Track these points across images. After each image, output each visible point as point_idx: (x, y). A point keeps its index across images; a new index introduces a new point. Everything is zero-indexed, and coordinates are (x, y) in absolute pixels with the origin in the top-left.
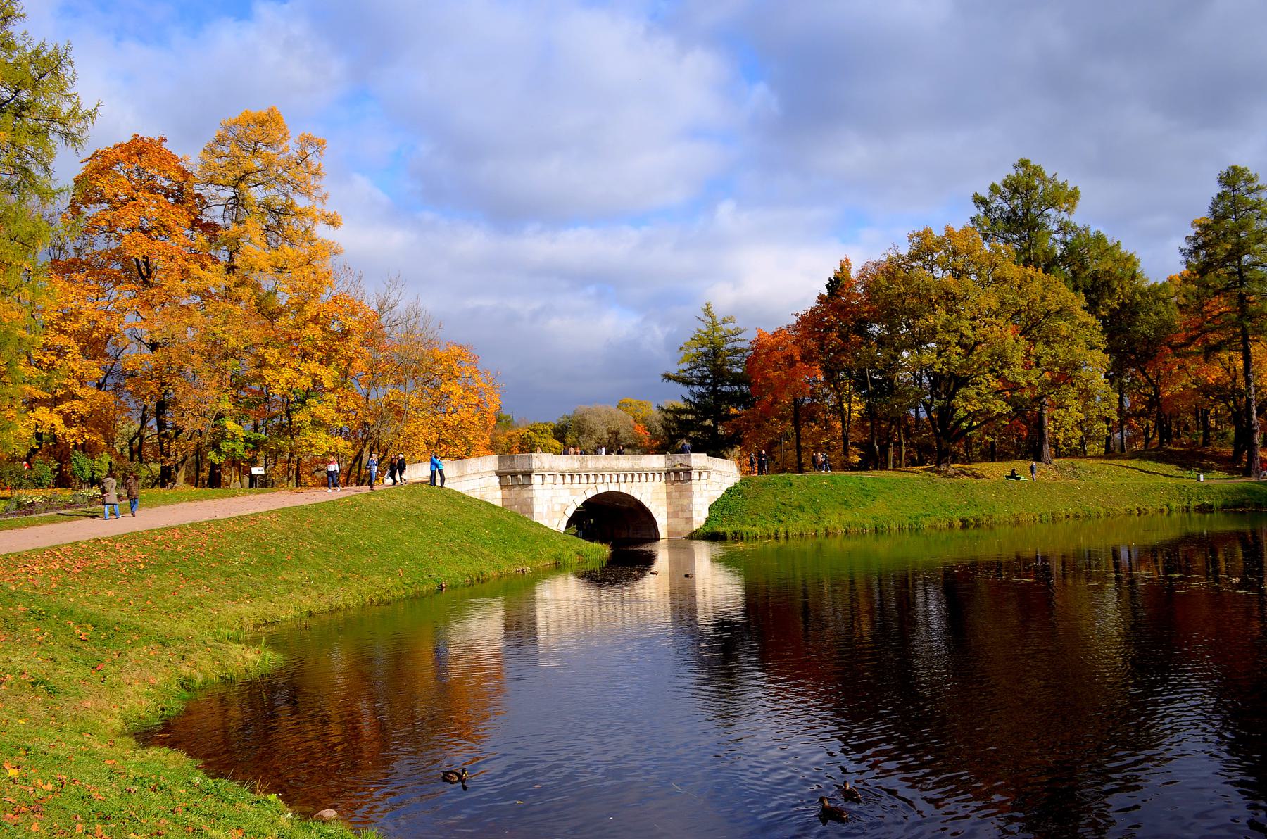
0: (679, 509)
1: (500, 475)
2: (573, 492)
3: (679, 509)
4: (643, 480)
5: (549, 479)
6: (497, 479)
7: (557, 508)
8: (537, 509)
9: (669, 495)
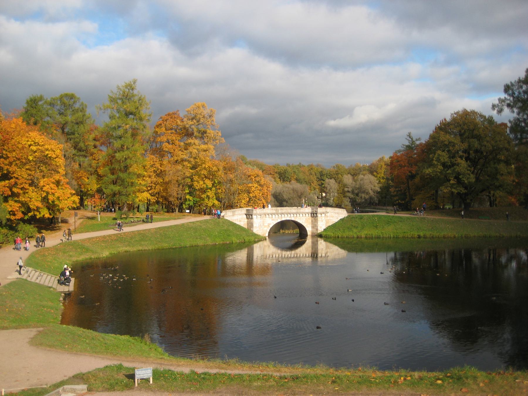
0: (315, 225)
1: (246, 215)
2: (273, 220)
3: (315, 225)
4: (302, 215)
7: (266, 224)
8: (254, 225)
9: (312, 221)
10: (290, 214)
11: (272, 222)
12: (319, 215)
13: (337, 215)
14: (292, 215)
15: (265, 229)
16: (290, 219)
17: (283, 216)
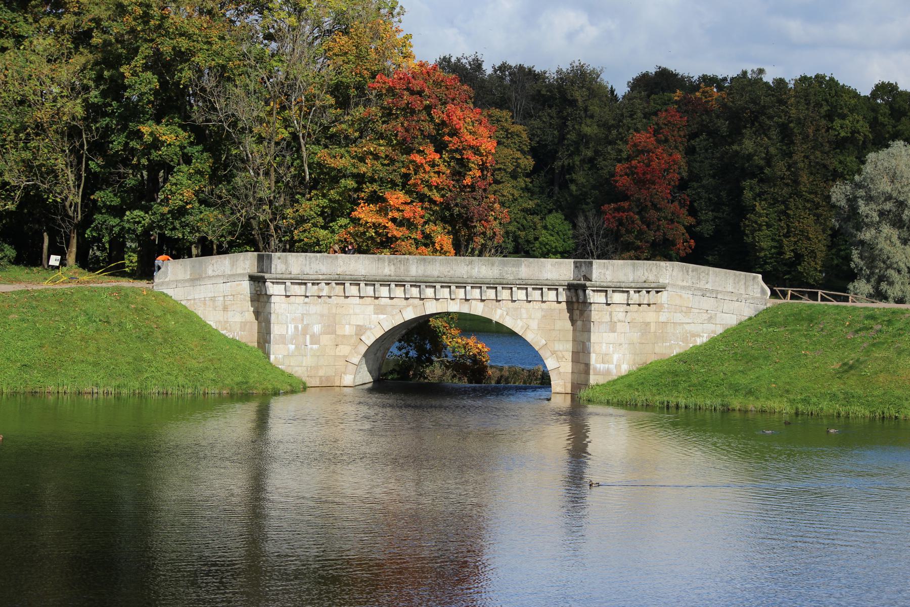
2: (380, 310)
7: (348, 330)
12: (596, 298)
13: (708, 303)
15: (344, 350)
16: (465, 309)
17: (429, 292)
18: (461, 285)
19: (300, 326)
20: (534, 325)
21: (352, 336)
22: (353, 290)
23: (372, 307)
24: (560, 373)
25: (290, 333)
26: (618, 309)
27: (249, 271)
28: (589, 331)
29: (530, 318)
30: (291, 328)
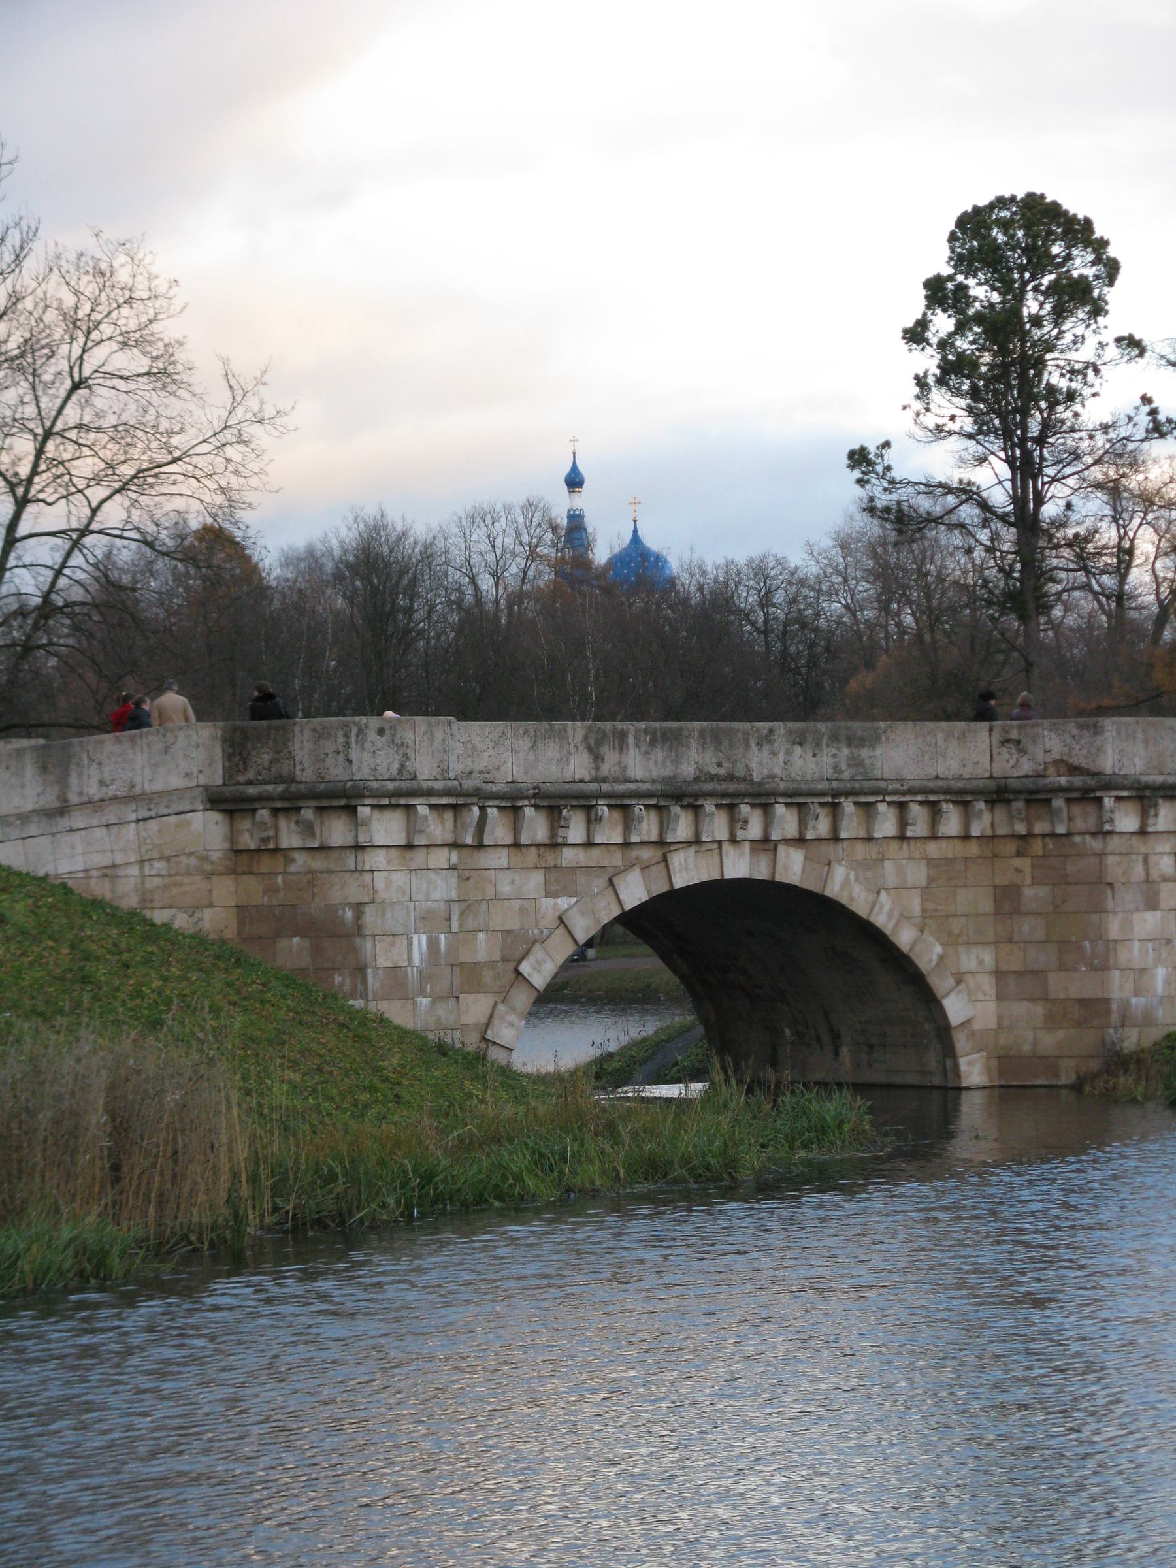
1: (228, 803)
2: (561, 881)
5: (438, 828)
6: (208, 830)
7: (483, 948)
8: (382, 955)
9: (1007, 900)
10: (763, 798)
11: (551, 906)
14: (786, 821)
18: (763, 798)
19: (442, 936)
20: (915, 904)
21: (491, 964)
22: (498, 829)
23: (536, 879)
24: (973, 1034)
25: (416, 961)
26: (1160, 849)
27: (202, 780)
28: (1100, 909)
29: (902, 887)
30: (420, 942)
